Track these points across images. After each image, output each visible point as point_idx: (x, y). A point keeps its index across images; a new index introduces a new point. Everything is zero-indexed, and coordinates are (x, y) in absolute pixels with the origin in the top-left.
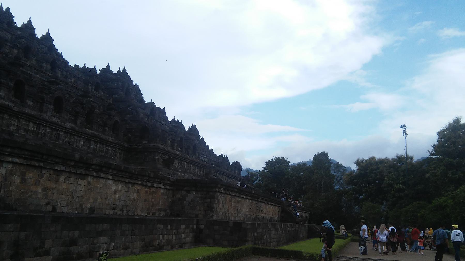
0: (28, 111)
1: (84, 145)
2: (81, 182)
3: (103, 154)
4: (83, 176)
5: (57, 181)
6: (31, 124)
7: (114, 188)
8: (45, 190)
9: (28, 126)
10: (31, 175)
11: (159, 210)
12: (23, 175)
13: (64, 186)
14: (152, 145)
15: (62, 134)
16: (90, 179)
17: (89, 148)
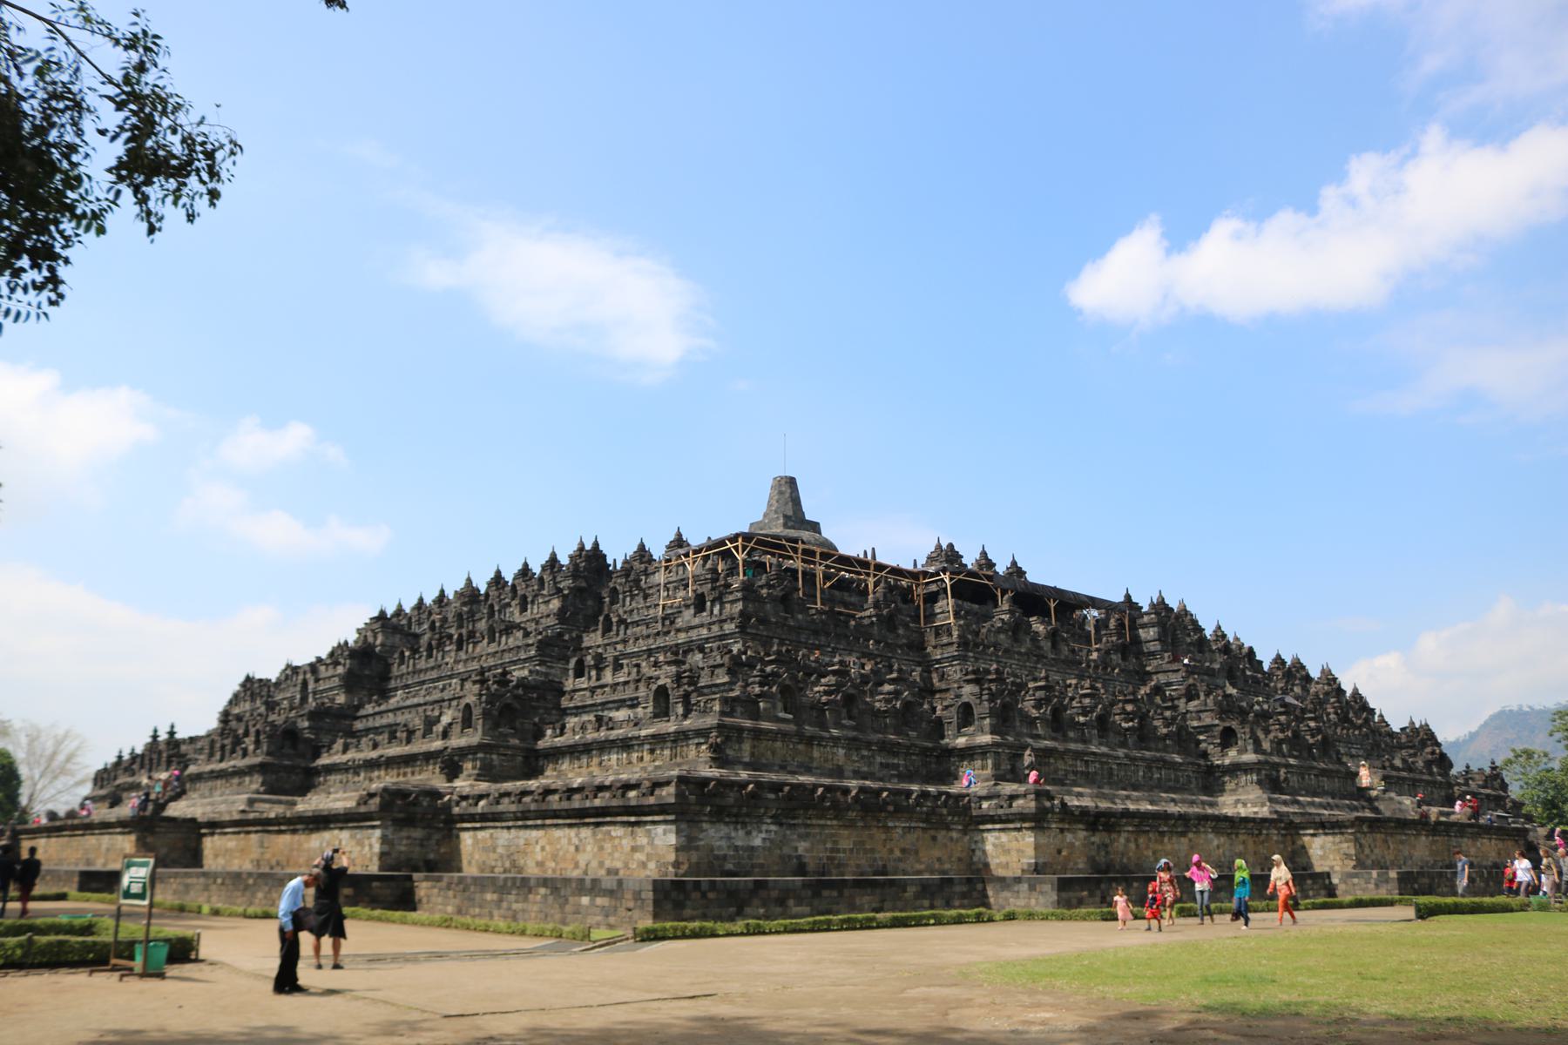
0: (1073, 746)
1: (1144, 777)
2: (1182, 839)
3: (1171, 784)
4: (1183, 834)
5: (1162, 842)
6: (1079, 763)
7: (1216, 842)
9: (1076, 766)
12: (1136, 840)
15: (1114, 767)
16: (1191, 835)
17: (1151, 778)
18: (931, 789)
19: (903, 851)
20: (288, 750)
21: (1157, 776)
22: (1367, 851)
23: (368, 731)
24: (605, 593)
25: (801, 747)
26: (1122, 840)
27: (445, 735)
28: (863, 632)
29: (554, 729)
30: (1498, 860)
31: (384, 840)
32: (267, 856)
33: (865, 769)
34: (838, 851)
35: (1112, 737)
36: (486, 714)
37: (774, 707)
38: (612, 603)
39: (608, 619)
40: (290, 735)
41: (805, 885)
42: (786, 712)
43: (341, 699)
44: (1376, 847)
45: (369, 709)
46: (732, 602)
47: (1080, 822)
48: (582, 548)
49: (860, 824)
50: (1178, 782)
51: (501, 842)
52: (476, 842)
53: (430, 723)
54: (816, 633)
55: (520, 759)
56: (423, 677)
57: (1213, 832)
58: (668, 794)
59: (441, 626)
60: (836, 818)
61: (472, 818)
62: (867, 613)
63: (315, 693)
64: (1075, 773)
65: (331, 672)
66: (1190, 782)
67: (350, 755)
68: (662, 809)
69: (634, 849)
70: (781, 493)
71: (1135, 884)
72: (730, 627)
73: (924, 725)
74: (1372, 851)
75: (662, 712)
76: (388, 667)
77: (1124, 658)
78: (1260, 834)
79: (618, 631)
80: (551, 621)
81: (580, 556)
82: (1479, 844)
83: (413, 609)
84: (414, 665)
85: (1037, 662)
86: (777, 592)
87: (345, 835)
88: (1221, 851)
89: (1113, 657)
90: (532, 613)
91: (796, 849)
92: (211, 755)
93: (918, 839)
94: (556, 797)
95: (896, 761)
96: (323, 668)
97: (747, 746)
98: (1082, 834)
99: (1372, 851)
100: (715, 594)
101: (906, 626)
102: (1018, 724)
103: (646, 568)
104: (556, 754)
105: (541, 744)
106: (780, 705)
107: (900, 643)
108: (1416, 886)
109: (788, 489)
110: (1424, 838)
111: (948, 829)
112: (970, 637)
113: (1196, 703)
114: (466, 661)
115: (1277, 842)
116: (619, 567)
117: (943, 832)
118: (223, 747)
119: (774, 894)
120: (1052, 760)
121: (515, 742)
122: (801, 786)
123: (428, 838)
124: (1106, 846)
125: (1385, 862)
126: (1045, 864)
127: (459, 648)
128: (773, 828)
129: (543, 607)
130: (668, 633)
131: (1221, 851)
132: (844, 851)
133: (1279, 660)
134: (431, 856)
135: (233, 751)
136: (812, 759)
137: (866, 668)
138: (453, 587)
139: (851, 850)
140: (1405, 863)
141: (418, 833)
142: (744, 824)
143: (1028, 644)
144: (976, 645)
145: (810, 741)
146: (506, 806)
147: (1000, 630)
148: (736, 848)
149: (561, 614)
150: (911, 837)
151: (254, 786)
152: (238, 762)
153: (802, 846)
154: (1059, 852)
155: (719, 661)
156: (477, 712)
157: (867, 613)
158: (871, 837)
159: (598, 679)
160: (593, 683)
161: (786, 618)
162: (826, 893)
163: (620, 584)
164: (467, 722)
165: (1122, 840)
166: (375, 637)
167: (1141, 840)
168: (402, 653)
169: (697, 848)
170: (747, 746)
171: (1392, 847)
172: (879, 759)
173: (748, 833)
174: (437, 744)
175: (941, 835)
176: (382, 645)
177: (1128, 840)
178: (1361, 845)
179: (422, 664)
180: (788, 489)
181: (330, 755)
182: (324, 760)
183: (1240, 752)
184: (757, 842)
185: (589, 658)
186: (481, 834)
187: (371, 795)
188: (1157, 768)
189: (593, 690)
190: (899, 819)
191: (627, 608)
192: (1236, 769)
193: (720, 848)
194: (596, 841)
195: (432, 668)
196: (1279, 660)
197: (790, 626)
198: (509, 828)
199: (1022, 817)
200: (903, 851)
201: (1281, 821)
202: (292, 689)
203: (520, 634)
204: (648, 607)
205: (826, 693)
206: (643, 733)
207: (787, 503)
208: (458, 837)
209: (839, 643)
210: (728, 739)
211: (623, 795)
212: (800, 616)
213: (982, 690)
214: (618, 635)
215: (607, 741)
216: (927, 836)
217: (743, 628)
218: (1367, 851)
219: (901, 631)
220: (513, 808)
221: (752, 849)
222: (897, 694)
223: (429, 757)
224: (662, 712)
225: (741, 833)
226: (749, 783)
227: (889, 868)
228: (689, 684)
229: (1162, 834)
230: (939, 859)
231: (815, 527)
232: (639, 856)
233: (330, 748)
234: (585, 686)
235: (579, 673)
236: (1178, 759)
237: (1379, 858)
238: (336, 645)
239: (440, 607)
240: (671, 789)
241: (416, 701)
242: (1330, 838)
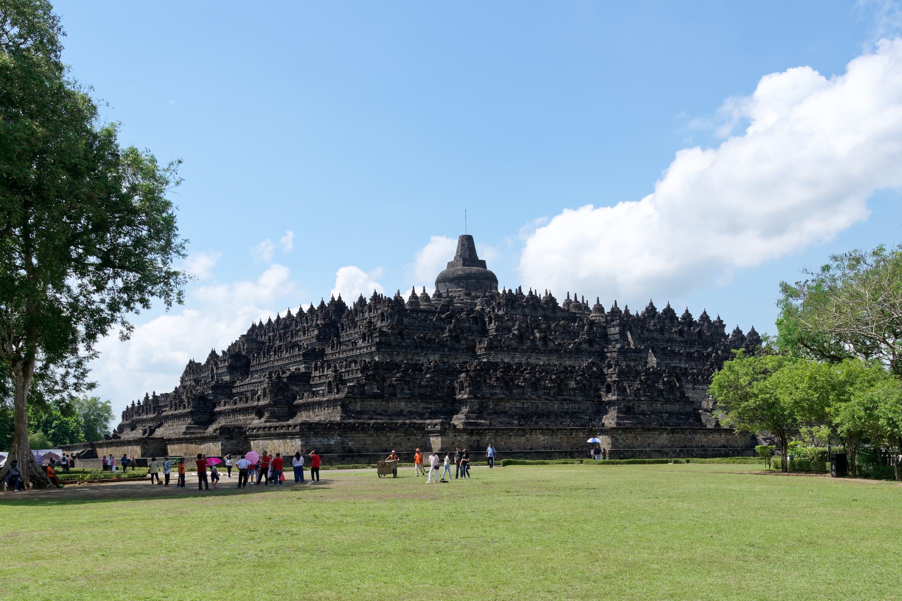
2: (522, 438)
3: (576, 410)
4: (523, 436)
6: (518, 404)
7: (543, 438)
8: (505, 443)
10: (498, 438)
11: (581, 447)
13: (514, 441)
18: (408, 422)
19: (394, 444)
22: (621, 441)
23: (238, 394)
24: (339, 325)
25: (383, 403)
26: (487, 439)
27: (259, 400)
28: (442, 345)
29: (299, 396)
30: (726, 444)
31: (222, 445)
32: (188, 451)
33: (415, 410)
34: (366, 445)
35: (541, 392)
36: (270, 391)
38: (343, 329)
39: (333, 341)
40: (202, 398)
41: (338, 456)
42: (378, 390)
43: (227, 378)
44: (628, 439)
45: (238, 384)
46: (376, 337)
47: (464, 432)
48: (333, 298)
49: (375, 435)
50: (580, 409)
51: (261, 444)
52: (254, 444)
53: (254, 393)
55: (286, 409)
56: (262, 367)
57: (541, 434)
58: (298, 429)
59: (273, 339)
60: (364, 433)
61: (252, 436)
62: (445, 335)
63: (217, 374)
65: (222, 365)
66: (589, 409)
67: (227, 407)
68: (297, 434)
69: (292, 446)
70: (463, 245)
71: (471, 455)
72: (374, 349)
73: (445, 390)
74: (624, 441)
75: (330, 392)
76: (249, 362)
78: (571, 434)
79: (337, 347)
80: (314, 340)
81: (332, 304)
82: (710, 437)
83: (266, 325)
84: (259, 360)
85: (533, 352)
86: (396, 331)
87: (211, 444)
88: (546, 442)
89: (583, 346)
90: (308, 335)
91: (348, 444)
92: (171, 407)
93: (401, 440)
94: (272, 429)
95: (430, 406)
96: (219, 362)
97: (359, 405)
98: (465, 437)
99: (624, 441)
100: (369, 334)
101: (466, 339)
102: (484, 389)
103: (362, 310)
104: (300, 407)
105: (296, 402)
106: (375, 387)
107: (462, 347)
108: (622, 456)
109: (467, 244)
110: (665, 435)
111: (415, 435)
112: (495, 343)
113: (612, 369)
114: (277, 360)
115: (583, 438)
116: (352, 308)
117: (414, 437)
118: (176, 404)
119: (326, 459)
120: (502, 403)
122: (350, 423)
123: (239, 443)
124: (478, 441)
125: (634, 446)
126: (446, 449)
127: (275, 354)
128: (338, 438)
129: (312, 333)
130: (353, 350)
131: (546, 442)
132: (368, 445)
134: (240, 450)
135: (180, 406)
136: (389, 407)
137: (432, 364)
138: (283, 315)
139: (371, 444)
140: (649, 446)
141: (235, 442)
142: (327, 437)
143: (529, 343)
144: (497, 347)
146: (261, 432)
147: (511, 339)
148: (324, 445)
149: (318, 337)
150: (398, 439)
151: (189, 421)
152: (181, 411)
153: (350, 444)
154: (454, 443)
155: (359, 367)
156: (268, 391)
157: (445, 335)
158: (380, 439)
159: (323, 372)
160: (321, 374)
161: (401, 342)
162: (346, 459)
163: (345, 321)
164: (265, 395)
165: (487, 439)
166: (244, 347)
167: (498, 438)
168: (254, 355)
169: (309, 446)
170: (359, 405)
171: (639, 439)
172: (421, 405)
173: (329, 440)
174: (255, 403)
175: (412, 438)
176: (247, 349)
177: (490, 439)
178: (616, 439)
179: (262, 361)
180: (467, 244)
181: (220, 407)
182: (217, 409)
183: (612, 396)
184: (332, 442)
185: (319, 363)
186: (255, 442)
187: (217, 429)
188: (567, 404)
189: (320, 377)
190: (392, 433)
191: (348, 333)
192: (611, 403)
193: (318, 445)
194: (284, 444)
195: (265, 363)
197: (402, 346)
198: (262, 439)
199: (438, 432)
200: (394, 444)
201: (585, 429)
202: (207, 373)
203: (297, 349)
204: (355, 333)
205: (396, 380)
206: (324, 399)
207: (466, 251)
208: (250, 443)
209: (428, 351)
210: (350, 402)
211: (288, 429)
212: (408, 341)
213: (467, 376)
214: (337, 349)
215: (314, 402)
216: (406, 438)
217: (378, 349)
218: (621, 441)
219: (463, 342)
220: (262, 432)
221: (330, 445)
222: (432, 379)
223: (253, 408)
224: (330, 392)
225: (326, 440)
226: (328, 423)
227: (388, 450)
228: (339, 380)
229: (511, 436)
230: (411, 447)
231: (483, 264)
232: (293, 448)
233: (220, 403)
234: (318, 375)
235: (316, 370)
236: (580, 399)
237: (629, 444)
238: (230, 345)
239: (278, 325)
240: (298, 428)
241: (255, 380)
242: (604, 436)
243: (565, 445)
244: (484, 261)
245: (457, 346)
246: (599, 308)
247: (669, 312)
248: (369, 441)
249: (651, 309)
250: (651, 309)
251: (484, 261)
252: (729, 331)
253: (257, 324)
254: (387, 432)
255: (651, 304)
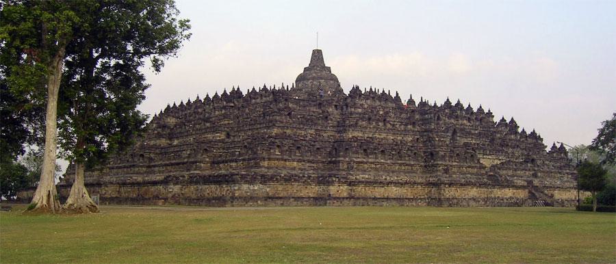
0: (370, 160)
10: (367, 188)
14: (436, 163)
20: (141, 160)
21: (403, 168)
22: (447, 192)
37: (275, 151)
54: (299, 124)
64: (371, 168)
69: (228, 190)
77: (414, 127)
121: (207, 159)
130: (255, 125)
133: (503, 120)
145: (285, 160)
150: (299, 187)
175: (309, 187)
180: (317, 55)
184: (256, 188)
196: (503, 120)
218: (447, 192)
243: (409, 194)
244: (330, 68)
245: (326, 124)
246: (411, 101)
247: (458, 104)
248: (280, 188)
249: (448, 102)
250: (448, 102)
251: (330, 68)
252: (497, 119)
253: (171, 106)
254: (293, 182)
255: (448, 100)
